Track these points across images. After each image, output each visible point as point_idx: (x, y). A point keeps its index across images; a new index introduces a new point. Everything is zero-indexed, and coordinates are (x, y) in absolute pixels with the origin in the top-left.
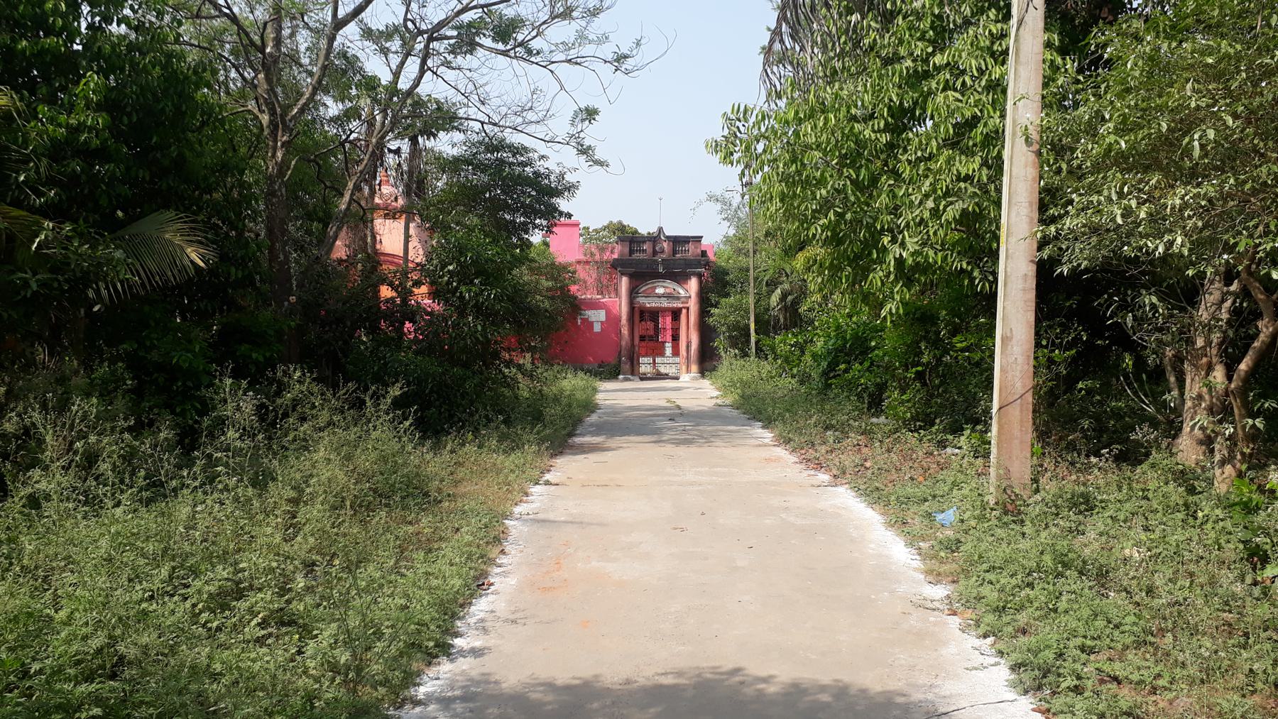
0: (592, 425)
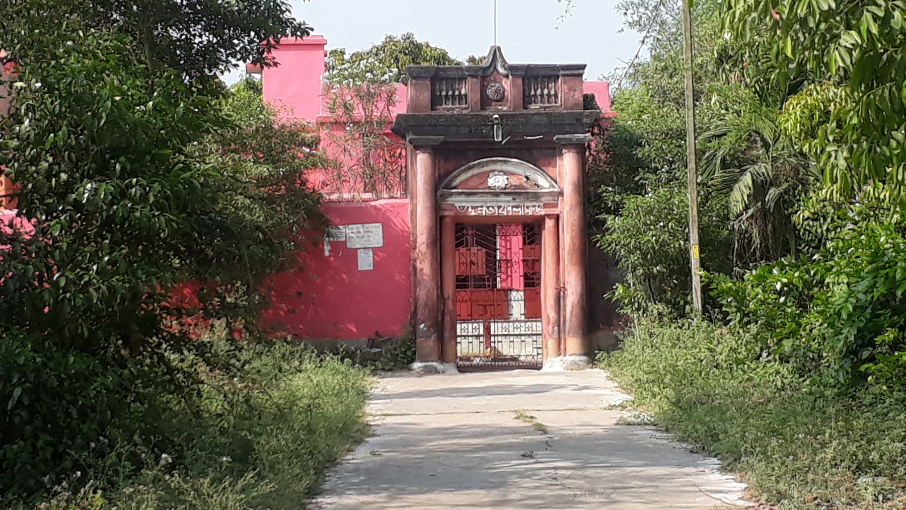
0: (356, 470)
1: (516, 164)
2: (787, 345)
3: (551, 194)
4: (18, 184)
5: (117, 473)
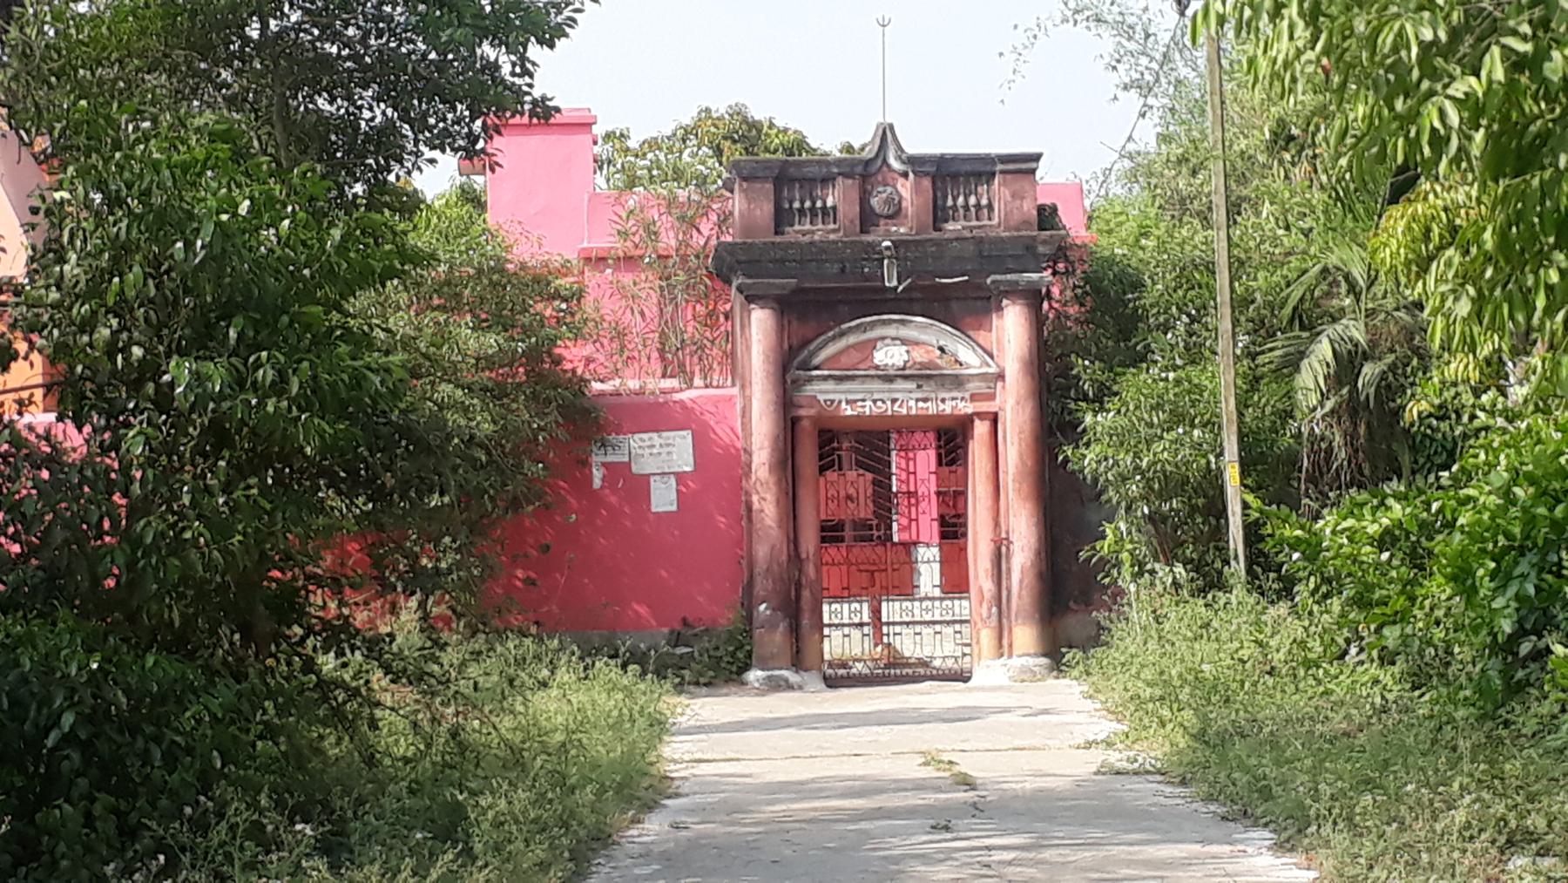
0: (646, 855)
1: (926, 326)
2: (1392, 634)
3: (983, 377)
4: (62, 367)
5: (229, 857)
